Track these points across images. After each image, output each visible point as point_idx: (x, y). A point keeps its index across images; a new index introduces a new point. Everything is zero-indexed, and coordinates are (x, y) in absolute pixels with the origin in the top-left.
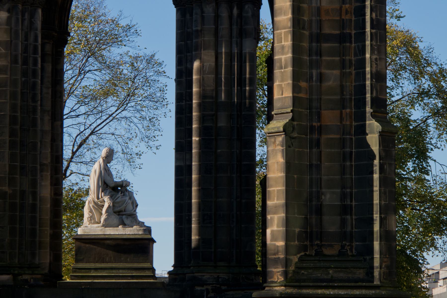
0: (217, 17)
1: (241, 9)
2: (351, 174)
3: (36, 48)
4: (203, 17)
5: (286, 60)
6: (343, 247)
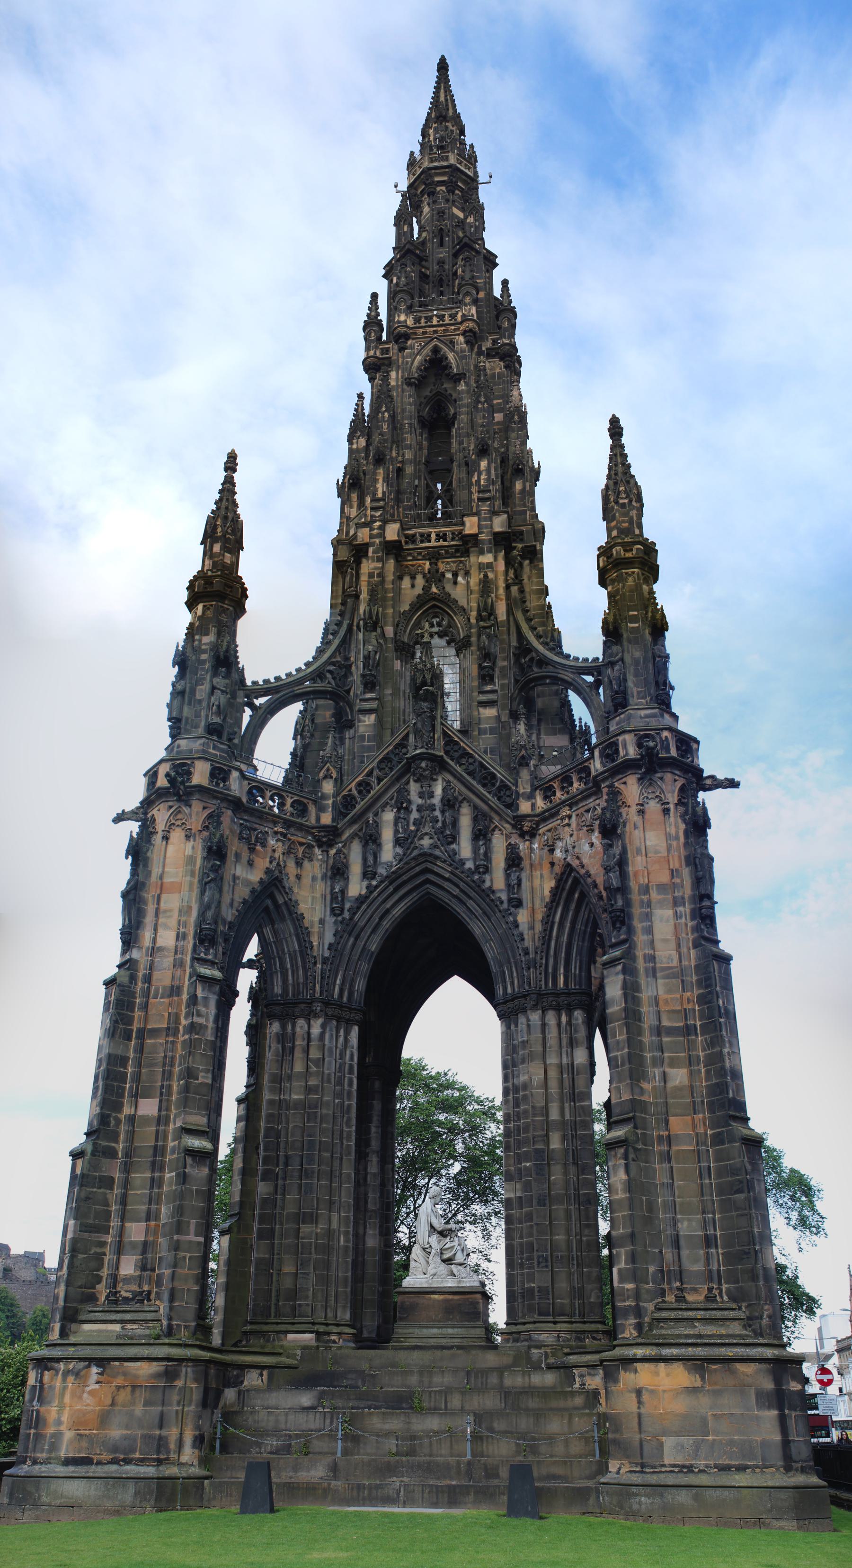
0: (544, 1025)
1: (570, 1016)
2: (712, 1195)
3: (351, 1066)
4: (529, 1026)
5: (622, 1056)
6: (710, 1290)
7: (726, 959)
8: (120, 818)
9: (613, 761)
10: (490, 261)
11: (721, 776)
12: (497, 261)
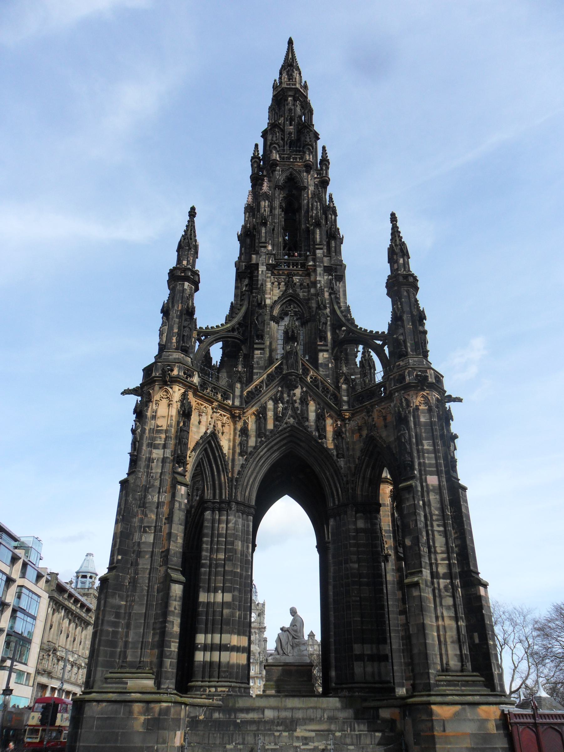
7: (464, 489)
8: (126, 392)
9: (401, 383)
10: (316, 136)
11: (454, 396)
12: (319, 137)
